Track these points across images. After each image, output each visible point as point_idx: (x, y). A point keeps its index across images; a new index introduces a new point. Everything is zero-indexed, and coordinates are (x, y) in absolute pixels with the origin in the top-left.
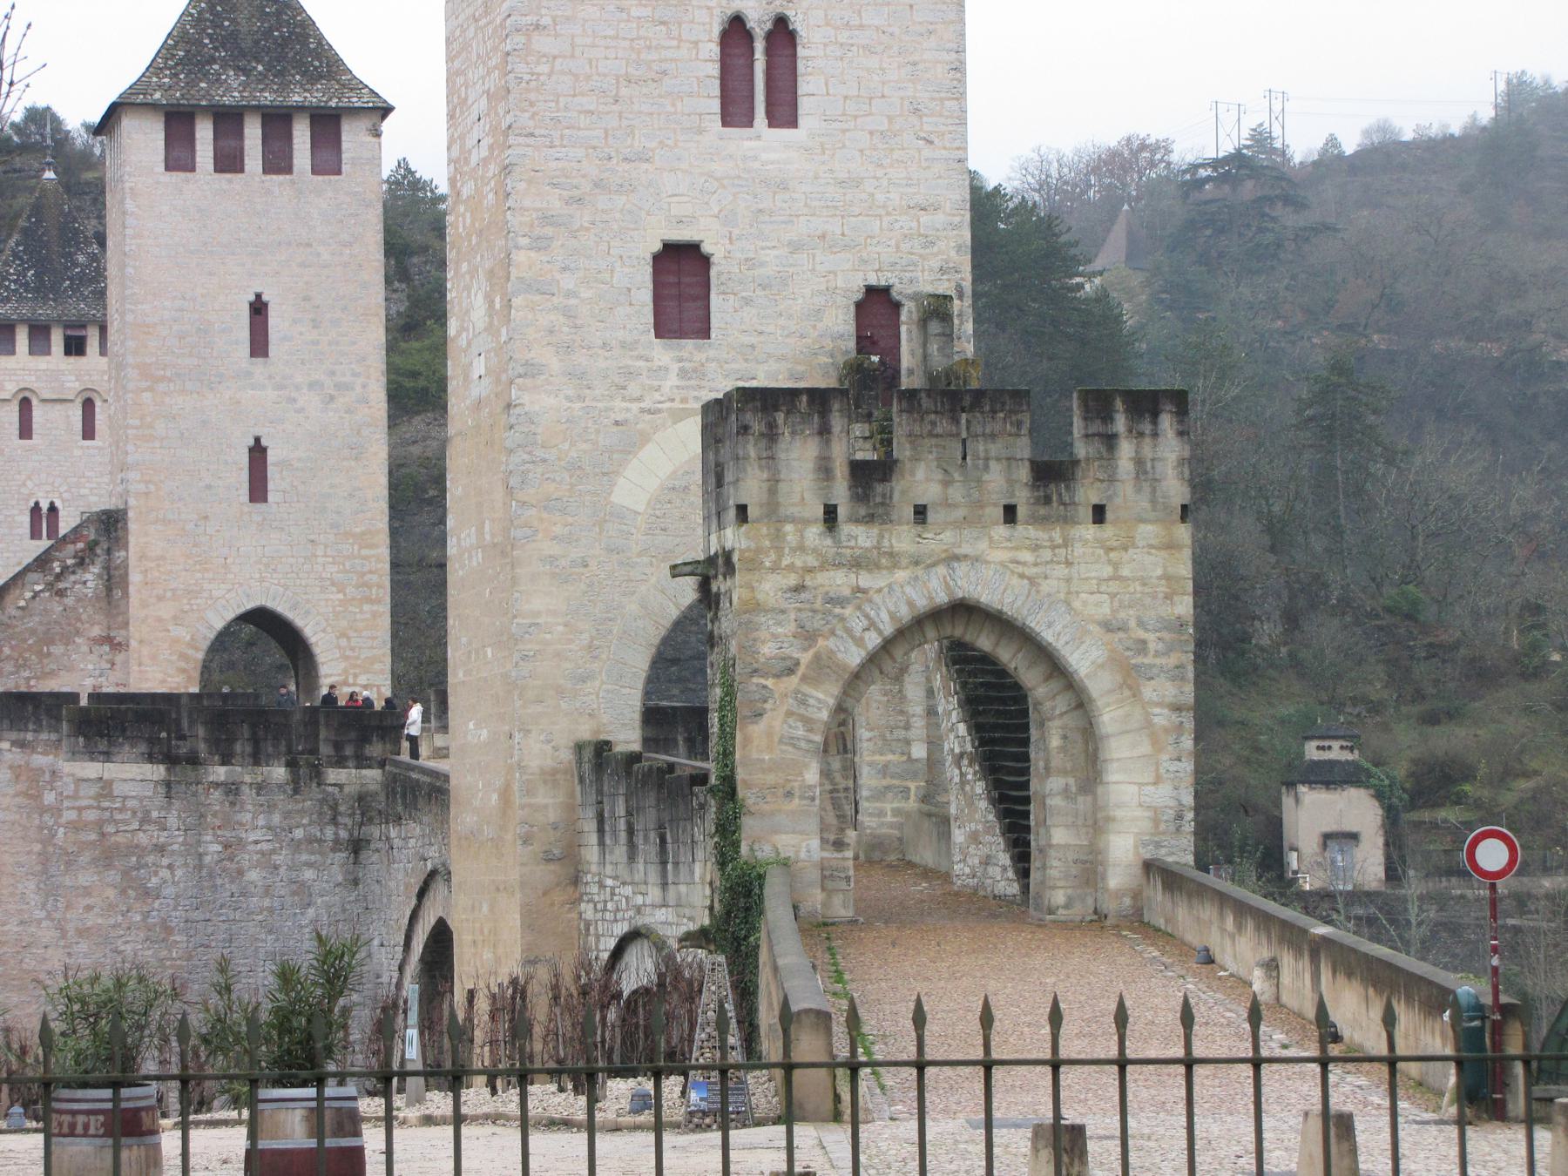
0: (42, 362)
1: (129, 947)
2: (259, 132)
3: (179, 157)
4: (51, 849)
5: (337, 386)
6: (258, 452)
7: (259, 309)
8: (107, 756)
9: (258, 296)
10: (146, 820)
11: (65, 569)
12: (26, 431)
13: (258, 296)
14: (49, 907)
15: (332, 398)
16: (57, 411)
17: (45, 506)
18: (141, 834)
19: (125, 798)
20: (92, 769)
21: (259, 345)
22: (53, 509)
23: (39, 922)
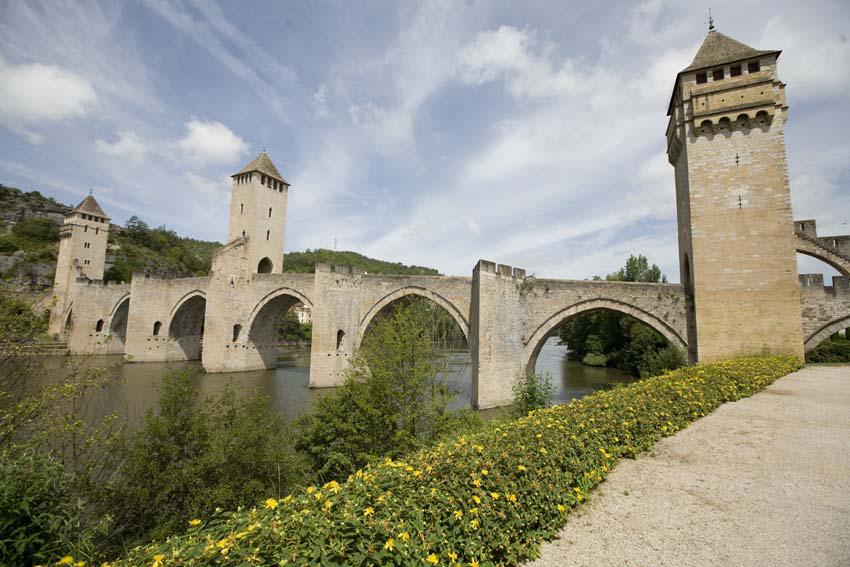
3: (263, 183)
20: (485, 273)
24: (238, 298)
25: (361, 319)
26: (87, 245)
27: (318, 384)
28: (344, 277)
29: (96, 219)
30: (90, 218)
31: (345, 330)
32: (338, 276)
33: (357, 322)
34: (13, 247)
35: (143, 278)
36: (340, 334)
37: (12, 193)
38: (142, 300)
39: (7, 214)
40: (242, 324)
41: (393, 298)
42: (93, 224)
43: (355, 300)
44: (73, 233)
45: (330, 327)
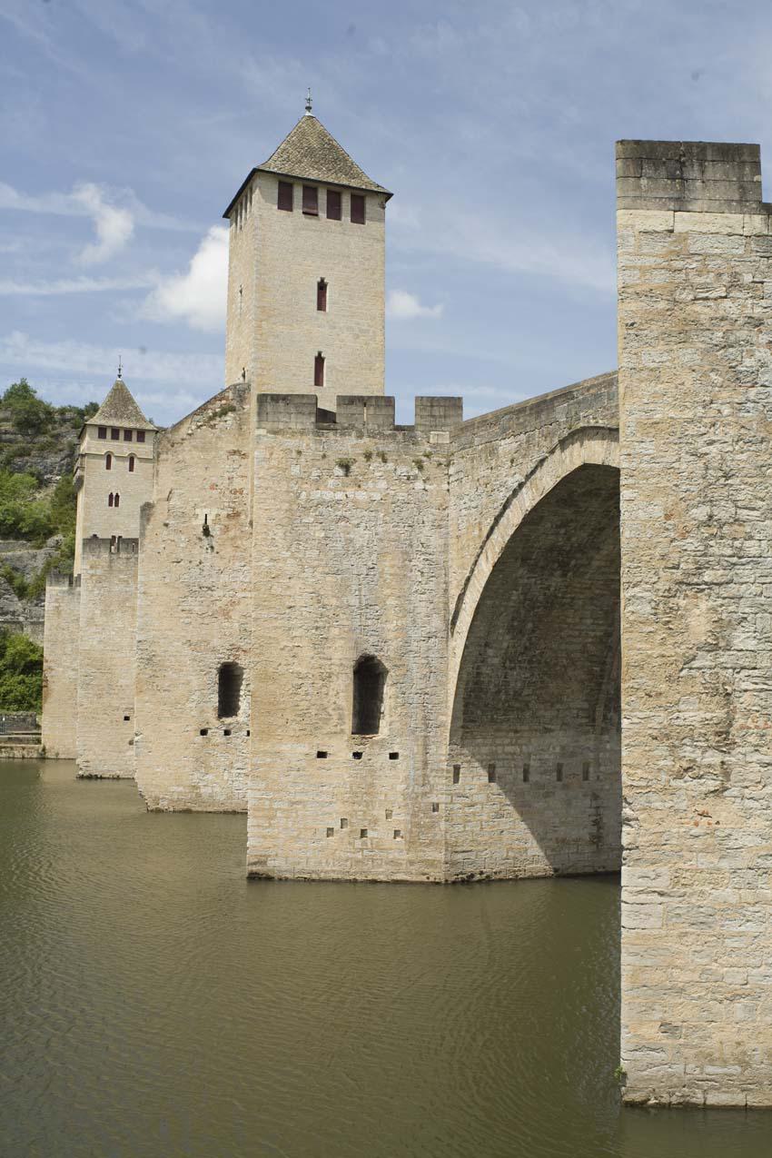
0: (115, 443)
1: (713, 449)
2: (325, 197)
4: (295, 507)
5: (361, 331)
6: (319, 361)
7: (322, 287)
8: (681, 204)
9: (322, 280)
10: (735, 284)
11: (215, 415)
12: (108, 467)
13: (322, 280)
14: (293, 549)
15: (358, 337)
16: (121, 463)
17: (114, 494)
18: (727, 303)
19: (707, 256)
20: (658, 219)
21: (321, 305)
22: (117, 496)
23: (285, 560)
24: (224, 578)
25: (452, 607)
26: (114, 500)
27: (277, 865)
28: (382, 445)
29: (128, 434)
30: (115, 433)
31: (387, 657)
32: (349, 445)
33: (437, 623)
34: (45, 526)
35: (106, 555)
36: (368, 676)
37: (57, 417)
38: (105, 613)
39: (49, 461)
40: (242, 662)
41: (528, 500)
42: (122, 448)
43: (425, 533)
44: (85, 474)
45: (320, 643)
